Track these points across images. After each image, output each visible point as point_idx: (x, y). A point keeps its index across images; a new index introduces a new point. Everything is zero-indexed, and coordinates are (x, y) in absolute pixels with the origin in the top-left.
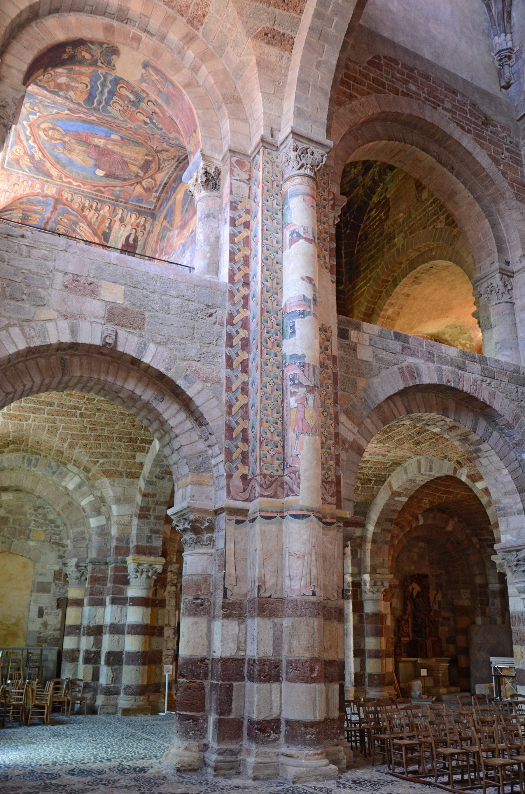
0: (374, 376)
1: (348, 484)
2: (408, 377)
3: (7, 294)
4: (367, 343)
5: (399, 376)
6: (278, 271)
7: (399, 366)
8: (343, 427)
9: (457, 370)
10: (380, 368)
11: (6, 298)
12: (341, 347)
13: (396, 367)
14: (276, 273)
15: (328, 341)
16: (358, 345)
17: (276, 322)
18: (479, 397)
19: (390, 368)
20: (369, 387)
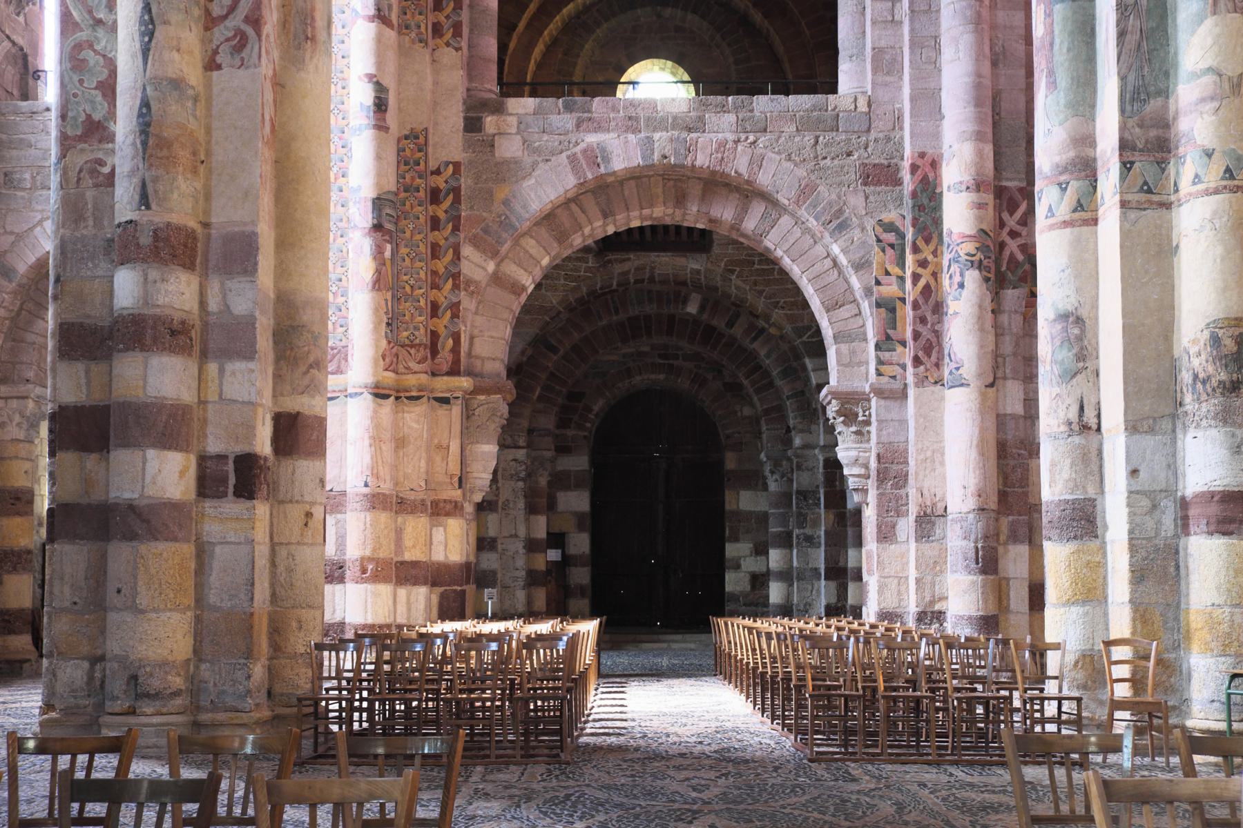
0: (524, 178)
1: (492, 337)
2: (585, 166)
3: (38, 183)
4: (514, 130)
5: (568, 169)
6: (345, 69)
7: (569, 153)
8: (467, 262)
9: (684, 134)
10: (534, 166)
11: (37, 188)
12: (468, 145)
13: (564, 155)
14: (342, 72)
15: (420, 151)
16: (496, 138)
17: (341, 144)
18: (727, 170)
19: (553, 159)
20: (514, 197)
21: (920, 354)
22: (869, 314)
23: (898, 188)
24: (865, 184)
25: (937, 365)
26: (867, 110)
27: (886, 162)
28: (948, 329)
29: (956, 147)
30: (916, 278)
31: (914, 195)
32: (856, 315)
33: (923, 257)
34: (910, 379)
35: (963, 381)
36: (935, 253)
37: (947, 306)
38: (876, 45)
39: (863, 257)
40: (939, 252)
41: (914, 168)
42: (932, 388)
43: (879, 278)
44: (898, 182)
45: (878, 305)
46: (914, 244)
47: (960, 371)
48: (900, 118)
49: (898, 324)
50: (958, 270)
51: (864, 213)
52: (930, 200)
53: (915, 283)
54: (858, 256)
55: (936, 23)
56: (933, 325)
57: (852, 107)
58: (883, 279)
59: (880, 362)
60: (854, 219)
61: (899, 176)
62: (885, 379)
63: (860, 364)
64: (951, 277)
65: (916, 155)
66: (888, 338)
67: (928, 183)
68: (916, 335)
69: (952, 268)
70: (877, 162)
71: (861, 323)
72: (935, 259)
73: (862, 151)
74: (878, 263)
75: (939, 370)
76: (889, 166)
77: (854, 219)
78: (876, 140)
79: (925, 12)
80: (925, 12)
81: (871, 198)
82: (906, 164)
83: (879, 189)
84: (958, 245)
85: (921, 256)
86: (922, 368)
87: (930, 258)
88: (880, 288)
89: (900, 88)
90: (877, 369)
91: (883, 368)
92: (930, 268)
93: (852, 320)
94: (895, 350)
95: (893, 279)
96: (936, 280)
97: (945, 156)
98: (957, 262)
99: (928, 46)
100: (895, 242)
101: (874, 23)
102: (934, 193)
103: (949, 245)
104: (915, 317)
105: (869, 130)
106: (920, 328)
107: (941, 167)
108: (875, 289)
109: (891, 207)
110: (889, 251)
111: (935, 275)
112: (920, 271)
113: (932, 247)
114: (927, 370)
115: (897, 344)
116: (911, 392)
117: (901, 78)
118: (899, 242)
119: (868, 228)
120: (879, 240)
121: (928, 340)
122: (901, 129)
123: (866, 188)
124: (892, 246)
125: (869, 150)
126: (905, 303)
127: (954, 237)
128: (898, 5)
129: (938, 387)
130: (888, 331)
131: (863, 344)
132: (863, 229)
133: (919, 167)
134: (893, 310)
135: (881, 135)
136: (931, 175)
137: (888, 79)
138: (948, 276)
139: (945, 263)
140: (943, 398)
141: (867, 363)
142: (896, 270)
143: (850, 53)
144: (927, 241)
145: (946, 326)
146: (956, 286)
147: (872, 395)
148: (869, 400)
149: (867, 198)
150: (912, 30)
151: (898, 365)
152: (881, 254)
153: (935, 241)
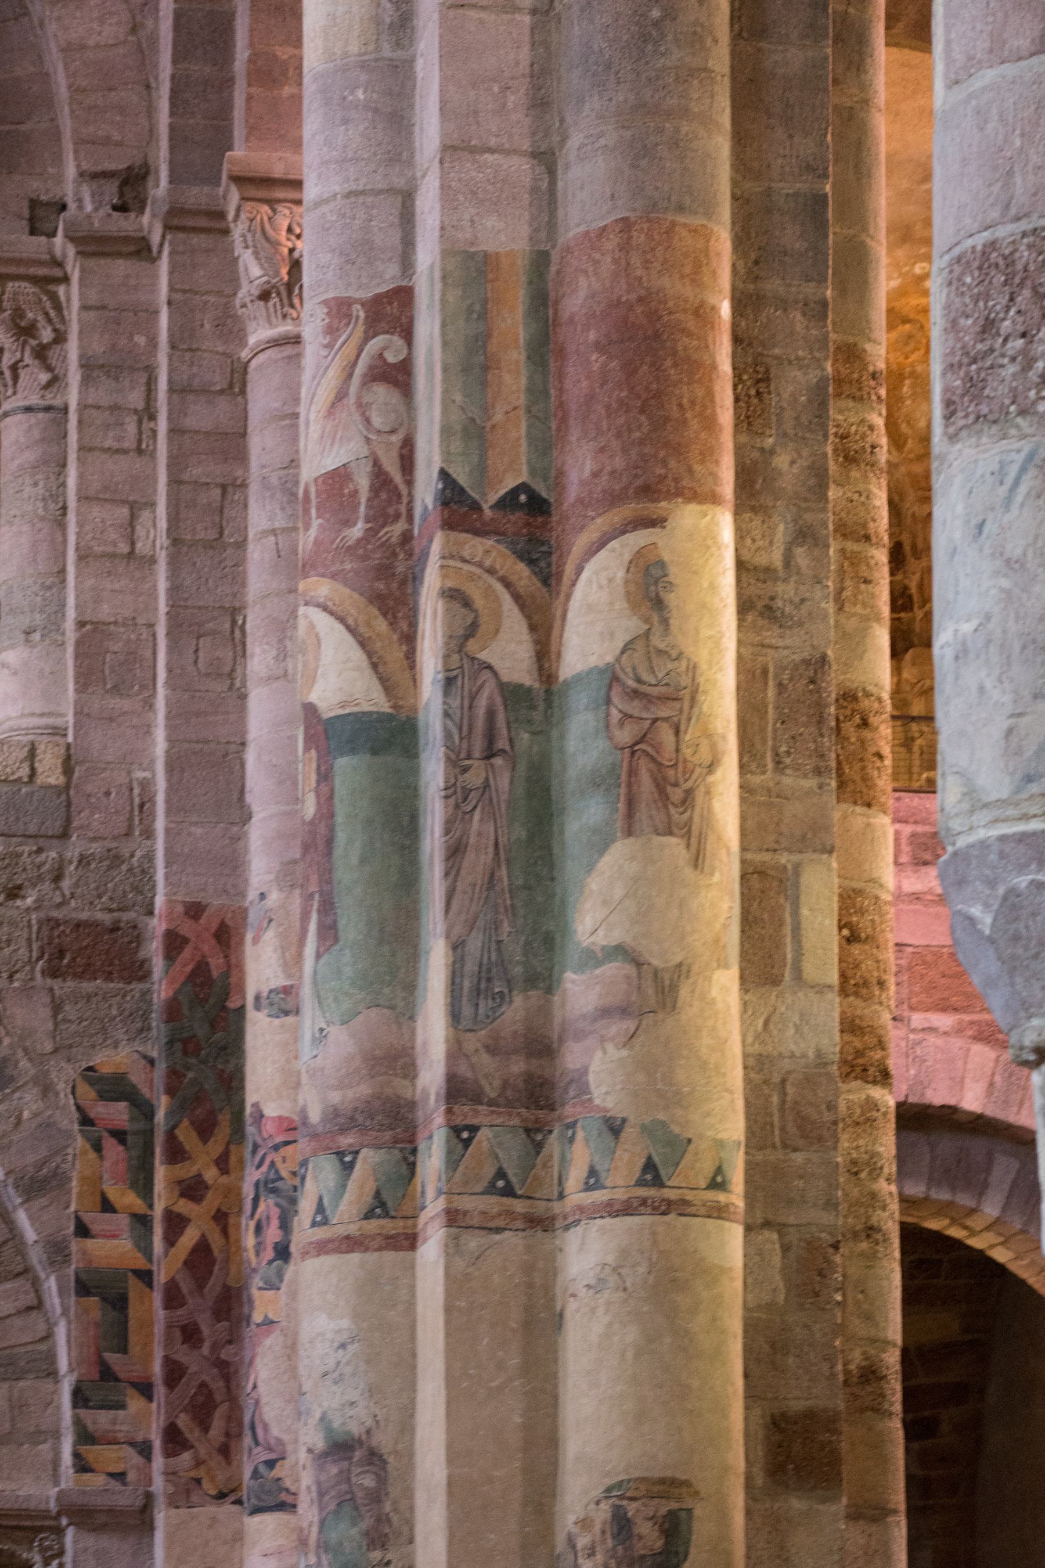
21: (183, 1421)
22: (59, 1310)
23: (137, 987)
24: (53, 972)
25: (225, 1451)
26: (62, 780)
27: (107, 918)
28: (251, 1363)
29: (274, 897)
30: (175, 1223)
31: (172, 1011)
32: (30, 1308)
33: (194, 1170)
34: (159, 1485)
35: (284, 1497)
36: (223, 1163)
37: (251, 1302)
38: (87, 618)
39: (44, 1162)
40: (233, 1159)
41: (174, 943)
42: (212, 1509)
43: (87, 1218)
44: (140, 972)
45: (83, 1288)
46: (171, 1136)
47: (276, 1473)
48: (146, 806)
49: (133, 1338)
50: (275, 1212)
51: (49, 1047)
52: (213, 1026)
53: (170, 1240)
54: (31, 1159)
55: (237, 577)
56: (215, 1347)
57: (24, 772)
58: (96, 1220)
59: (85, 1436)
60: (24, 1063)
61: (142, 954)
62: (97, 1481)
63: (38, 1436)
64: (259, 1229)
65: (180, 909)
66: (107, 1374)
67: (209, 981)
68: (174, 1373)
69: (262, 1207)
70: (84, 916)
71: (41, 1328)
72: (224, 1179)
73: (47, 886)
74: (83, 1179)
75: (229, 1463)
76: (115, 929)
77: (24, 1063)
78: (84, 861)
79: (208, 545)
80: (208, 545)
81: (70, 1011)
82: (157, 926)
83: (88, 986)
84: (276, 1148)
85: (186, 1171)
86: (186, 1457)
87: (210, 1174)
88: (89, 1243)
89: (147, 730)
90: (76, 1455)
91: (92, 1452)
92: (212, 1202)
93: (18, 1322)
94: (121, 1406)
95: (123, 1221)
96: (225, 1232)
97: (252, 917)
98: (274, 1191)
99: (213, 633)
100: (127, 1126)
101: (82, 558)
102: (224, 1008)
103: (256, 1147)
104: (169, 1326)
105: (64, 835)
106: (183, 1354)
107: (241, 942)
108: (75, 1246)
109: (120, 1034)
110: (113, 1149)
111: (221, 1218)
112: (184, 1207)
113: (215, 1147)
114: (199, 1463)
115: (131, 1391)
116: (161, 1517)
117: (149, 704)
118: (140, 1126)
119: (61, 1086)
120: (86, 1121)
121: (203, 1385)
122: (149, 834)
123: (56, 984)
124: (120, 1136)
125: (66, 884)
126: (150, 1285)
127: (269, 1128)
128: (145, 515)
129: (228, 1508)
130: (108, 1356)
131: (48, 1385)
132: (47, 1090)
133: (185, 941)
134: (119, 1303)
135: (96, 848)
136: (216, 963)
137: (115, 703)
138: (252, 1224)
139: (248, 1191)
140: (238, 1537)
141: (56, 1435)
142: (128, 1199)
143: (25, 621)
144: (205, 1130)
145: (247, 1354)
146: (269, 1253)
147: (64, 1521)
148: (60, 1531)
149: (57, 1008)
150: (174, 590)
151: (132, 1444)
152: (92, 1155)
153: (223, 1131)
